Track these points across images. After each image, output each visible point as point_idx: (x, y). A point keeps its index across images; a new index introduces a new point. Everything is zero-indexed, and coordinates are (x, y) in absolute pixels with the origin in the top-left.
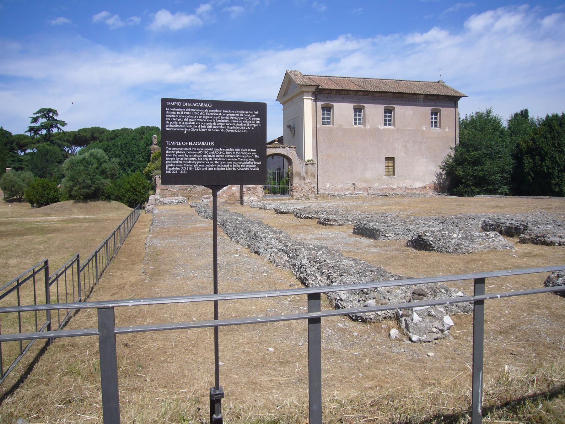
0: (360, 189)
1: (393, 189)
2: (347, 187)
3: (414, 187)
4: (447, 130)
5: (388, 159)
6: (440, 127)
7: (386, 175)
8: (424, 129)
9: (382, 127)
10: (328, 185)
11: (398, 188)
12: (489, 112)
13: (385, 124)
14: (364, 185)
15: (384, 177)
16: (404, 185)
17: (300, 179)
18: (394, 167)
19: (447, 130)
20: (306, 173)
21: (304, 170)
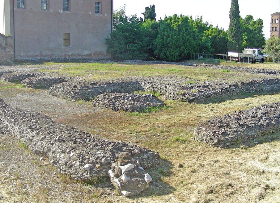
0: (46, 56)
1: (69, 56)
2: (36, 54)
3: (83, 54)
4: (106, 15)
5: (65, 33)
6: (101, 14)
7: (64, 46)
8: (91, 14)
9: (61, 11)
10: (22, 53)
11: (73, 55)
12: (150, 12)
13: (64, 10)
14: (48, 53)
15: (63, 47)
16: (77, 52)
17: (2, 49)
18: (69, 39)
19: (106, 15)
20: (6, 44)
21: (5, 42)
